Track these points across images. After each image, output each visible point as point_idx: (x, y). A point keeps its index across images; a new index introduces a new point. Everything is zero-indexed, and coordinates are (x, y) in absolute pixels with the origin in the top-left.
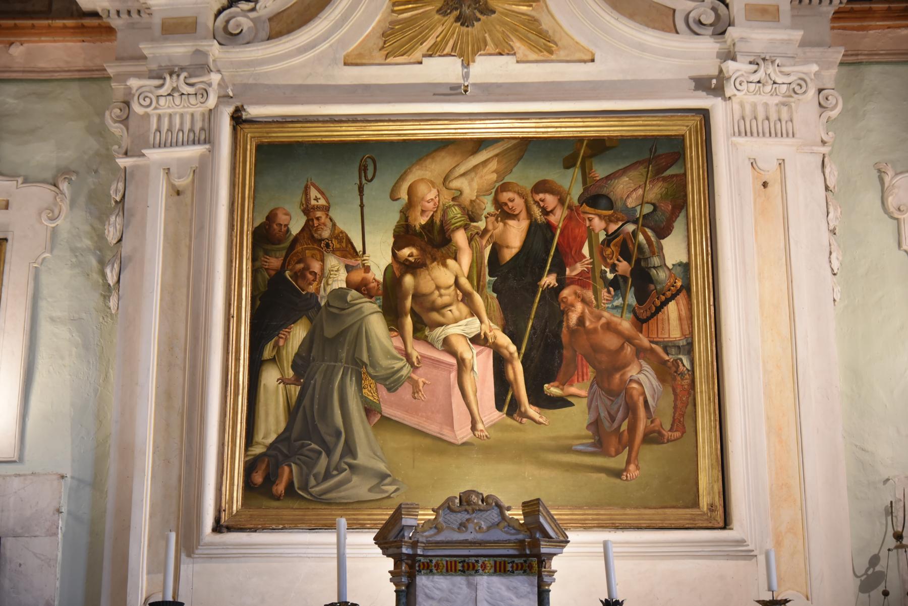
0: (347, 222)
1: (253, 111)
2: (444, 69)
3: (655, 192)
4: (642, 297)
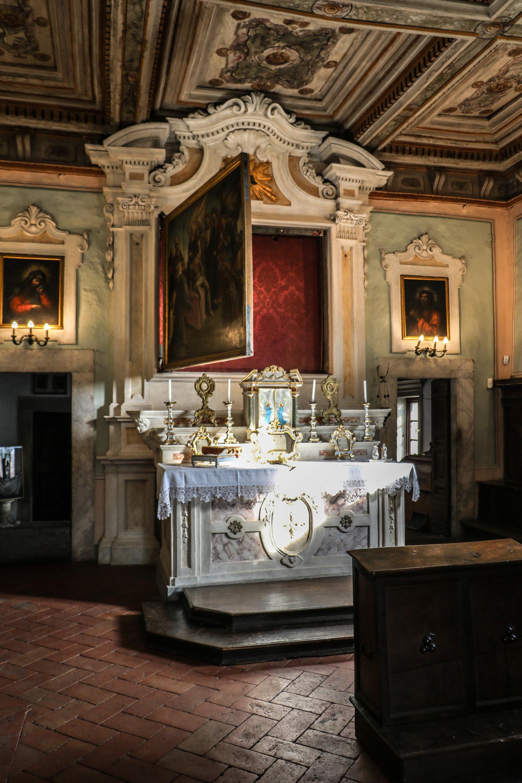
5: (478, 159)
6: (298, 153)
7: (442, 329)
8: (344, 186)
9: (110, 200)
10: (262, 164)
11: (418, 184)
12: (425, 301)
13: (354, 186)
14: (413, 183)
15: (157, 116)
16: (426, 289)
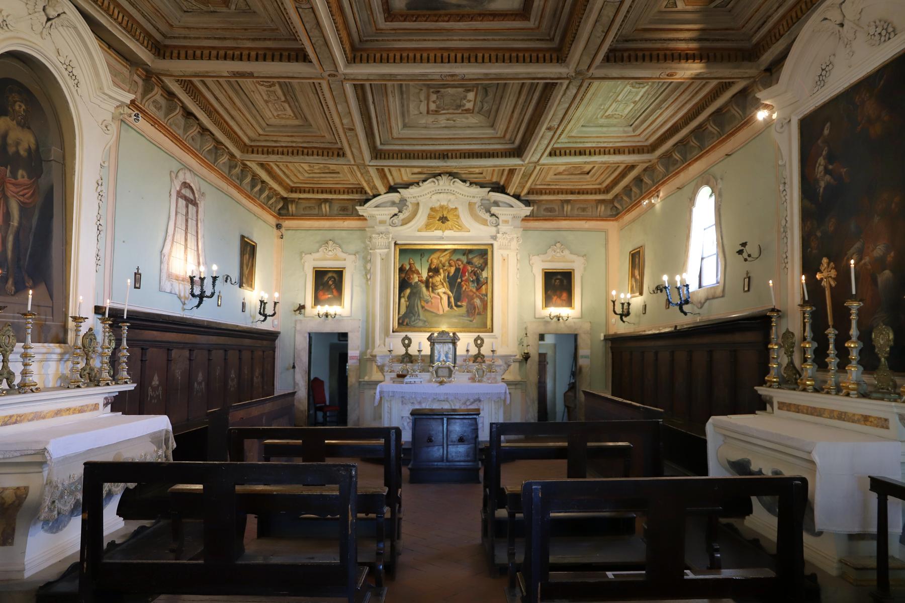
0: (418, 266)
1: (398, 242)
2: (438, 233)
3: (482, 261)
4: (478, 284)
6: (475, 200)
7: (569, 303)
8: (501, 218)
9: (369, 234)
10: (452, 209)
11: (555, 211)
12: (558, 284)
14: (551, 210)
15: (392, 189)
16: (559, 277)
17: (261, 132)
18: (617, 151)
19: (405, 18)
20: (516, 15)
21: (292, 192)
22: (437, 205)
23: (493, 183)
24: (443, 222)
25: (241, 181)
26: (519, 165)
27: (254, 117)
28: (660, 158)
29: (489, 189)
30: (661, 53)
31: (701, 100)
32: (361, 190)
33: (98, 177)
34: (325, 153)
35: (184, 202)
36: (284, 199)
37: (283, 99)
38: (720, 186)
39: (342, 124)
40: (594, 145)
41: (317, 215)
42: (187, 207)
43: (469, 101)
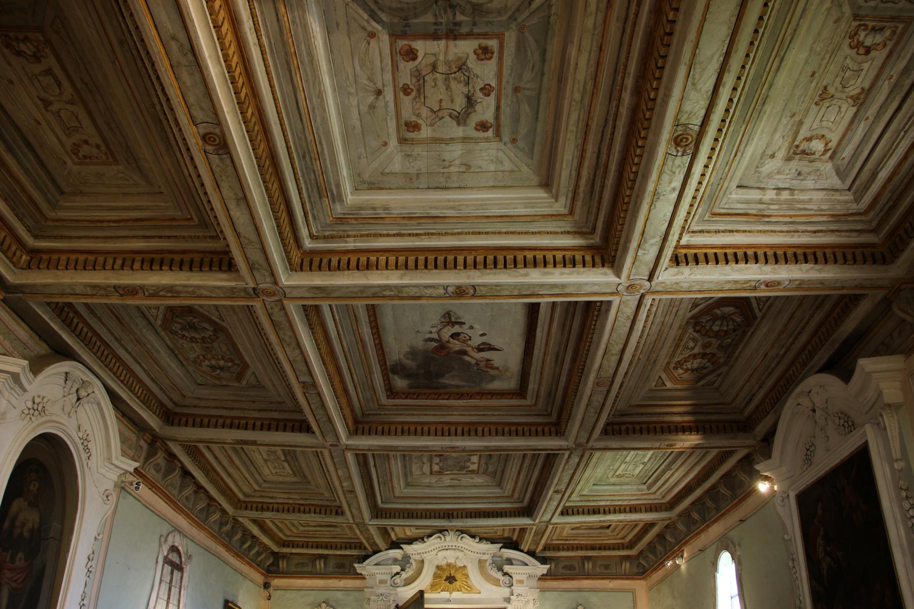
2: (445, 595)
5: (614, 549)
6: (485, 557)
8: (515, 577)
11: (575, 569)
13: (524, 577)
14: (570, 568)
17: (257, 488)
18: (633, 509)
19: (407, 395)
20: (514, 394)
21: (284, 546)
22: (443, 563)
23: (505, 538)
24: (451, 583)
25: (231, 538)
26: (530, 525)
27: (252, 474)
28: (680, 515)
29: (500, 545)
30: (658, 426)
31: (709, 463)
32: (360, 546)
33: (91, 552)
34: (323, 511)
35: (170, 568)
36: (274, 553)
37: (283, 458)
38: (738, 553)
39: (342, 487)
40: (608, 503)
41: (308, 573)
42: (172, 573)
43: (474, 463)
